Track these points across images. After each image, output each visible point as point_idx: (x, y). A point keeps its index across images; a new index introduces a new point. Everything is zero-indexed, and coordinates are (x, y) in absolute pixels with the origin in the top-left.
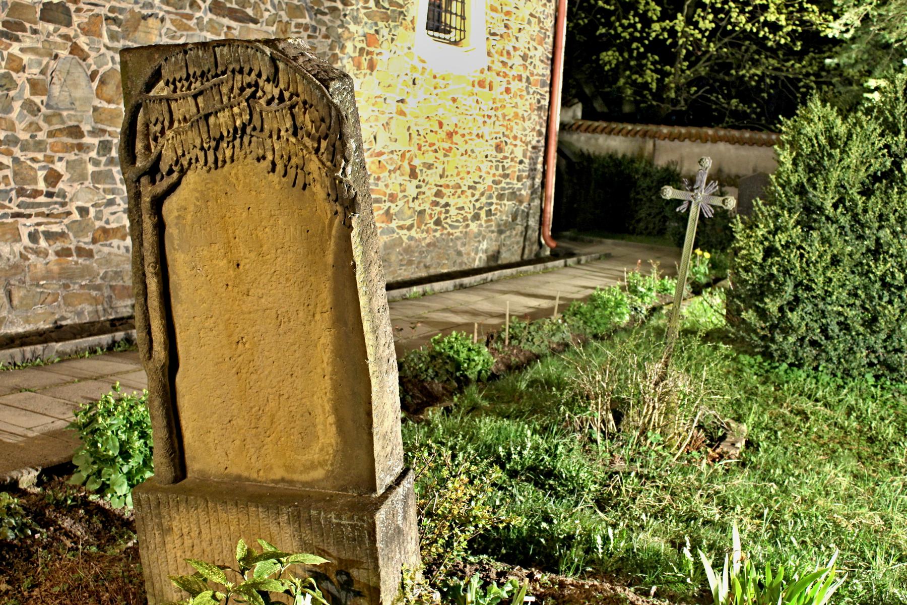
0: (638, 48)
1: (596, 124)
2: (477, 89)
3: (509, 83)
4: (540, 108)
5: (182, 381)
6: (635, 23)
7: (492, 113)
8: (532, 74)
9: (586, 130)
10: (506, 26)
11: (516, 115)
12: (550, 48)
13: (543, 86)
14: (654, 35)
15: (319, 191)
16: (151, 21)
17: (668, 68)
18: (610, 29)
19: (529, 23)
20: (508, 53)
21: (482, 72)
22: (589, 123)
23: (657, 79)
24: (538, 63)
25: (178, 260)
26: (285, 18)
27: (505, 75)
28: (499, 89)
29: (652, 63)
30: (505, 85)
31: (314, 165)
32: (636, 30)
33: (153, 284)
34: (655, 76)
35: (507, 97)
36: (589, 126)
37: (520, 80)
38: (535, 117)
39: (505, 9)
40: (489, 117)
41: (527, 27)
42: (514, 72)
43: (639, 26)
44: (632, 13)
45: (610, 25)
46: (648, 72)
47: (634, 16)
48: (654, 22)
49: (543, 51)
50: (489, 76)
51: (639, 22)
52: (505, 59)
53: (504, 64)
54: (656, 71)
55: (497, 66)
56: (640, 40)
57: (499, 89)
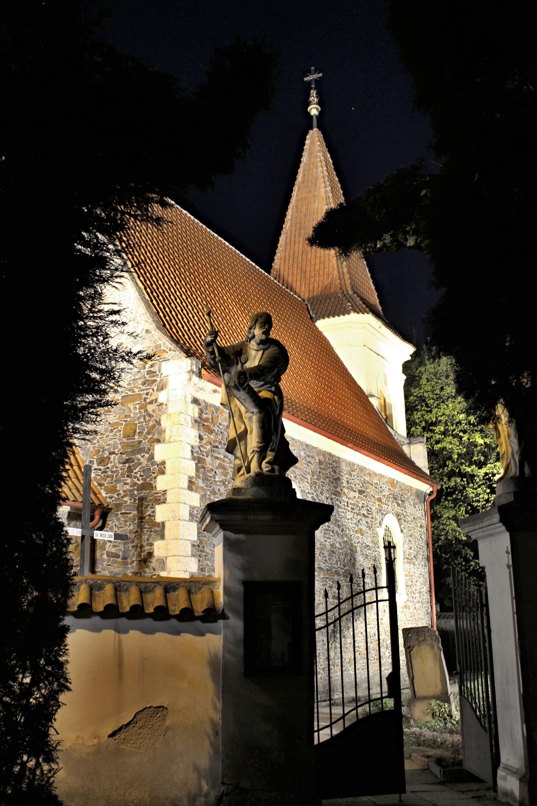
0: (465, 575)
1: (448, 614)
2: (404, 610)
3: (415, 605)
4: (428, 613)
5: (414, 681)
6: (462, 562)
7: (411, 619)
8: (423, 599)
9: (444, 618)
10: (412, 581)
11: (419, 618)
12: (428, 586)
13: (428, 603)
14: (472, 568)
15: (436, 648)
16: (321, 605)
17: (481, 583)
18: (449, 565)
19: (420, 577)
20: (414, 592)
21: (405, 602)
22: (445, 614)
23: (477, 589)
24: (425, 594)
25: (414, 662)
27: (414, 602)
28: (412, 608)
29: (473, 581)
30: (414, 606)
31: (435, 644)
32: (463, 566)
33: (410, 665)
34: (476, 588)
35: (415, 611)
36: (445, 615)
37: (419, 603)
38: (426, 618)
39: (411, 574)
40: (410, 621)
41: (419, 579)
42: (416, 600)
43: (464, 563)
44: (459, 557)
45: (449, 564)
46: (472, 586)
47: (460, 558)
48: (471, 561)
49: (426, 588)
50: (409, 604)
51: (464, 561)
52: (412, 595)
53: (413, 597)
54: (475, 585)
55: (410, 599)
56: (466, 570)
57: (412, 608)
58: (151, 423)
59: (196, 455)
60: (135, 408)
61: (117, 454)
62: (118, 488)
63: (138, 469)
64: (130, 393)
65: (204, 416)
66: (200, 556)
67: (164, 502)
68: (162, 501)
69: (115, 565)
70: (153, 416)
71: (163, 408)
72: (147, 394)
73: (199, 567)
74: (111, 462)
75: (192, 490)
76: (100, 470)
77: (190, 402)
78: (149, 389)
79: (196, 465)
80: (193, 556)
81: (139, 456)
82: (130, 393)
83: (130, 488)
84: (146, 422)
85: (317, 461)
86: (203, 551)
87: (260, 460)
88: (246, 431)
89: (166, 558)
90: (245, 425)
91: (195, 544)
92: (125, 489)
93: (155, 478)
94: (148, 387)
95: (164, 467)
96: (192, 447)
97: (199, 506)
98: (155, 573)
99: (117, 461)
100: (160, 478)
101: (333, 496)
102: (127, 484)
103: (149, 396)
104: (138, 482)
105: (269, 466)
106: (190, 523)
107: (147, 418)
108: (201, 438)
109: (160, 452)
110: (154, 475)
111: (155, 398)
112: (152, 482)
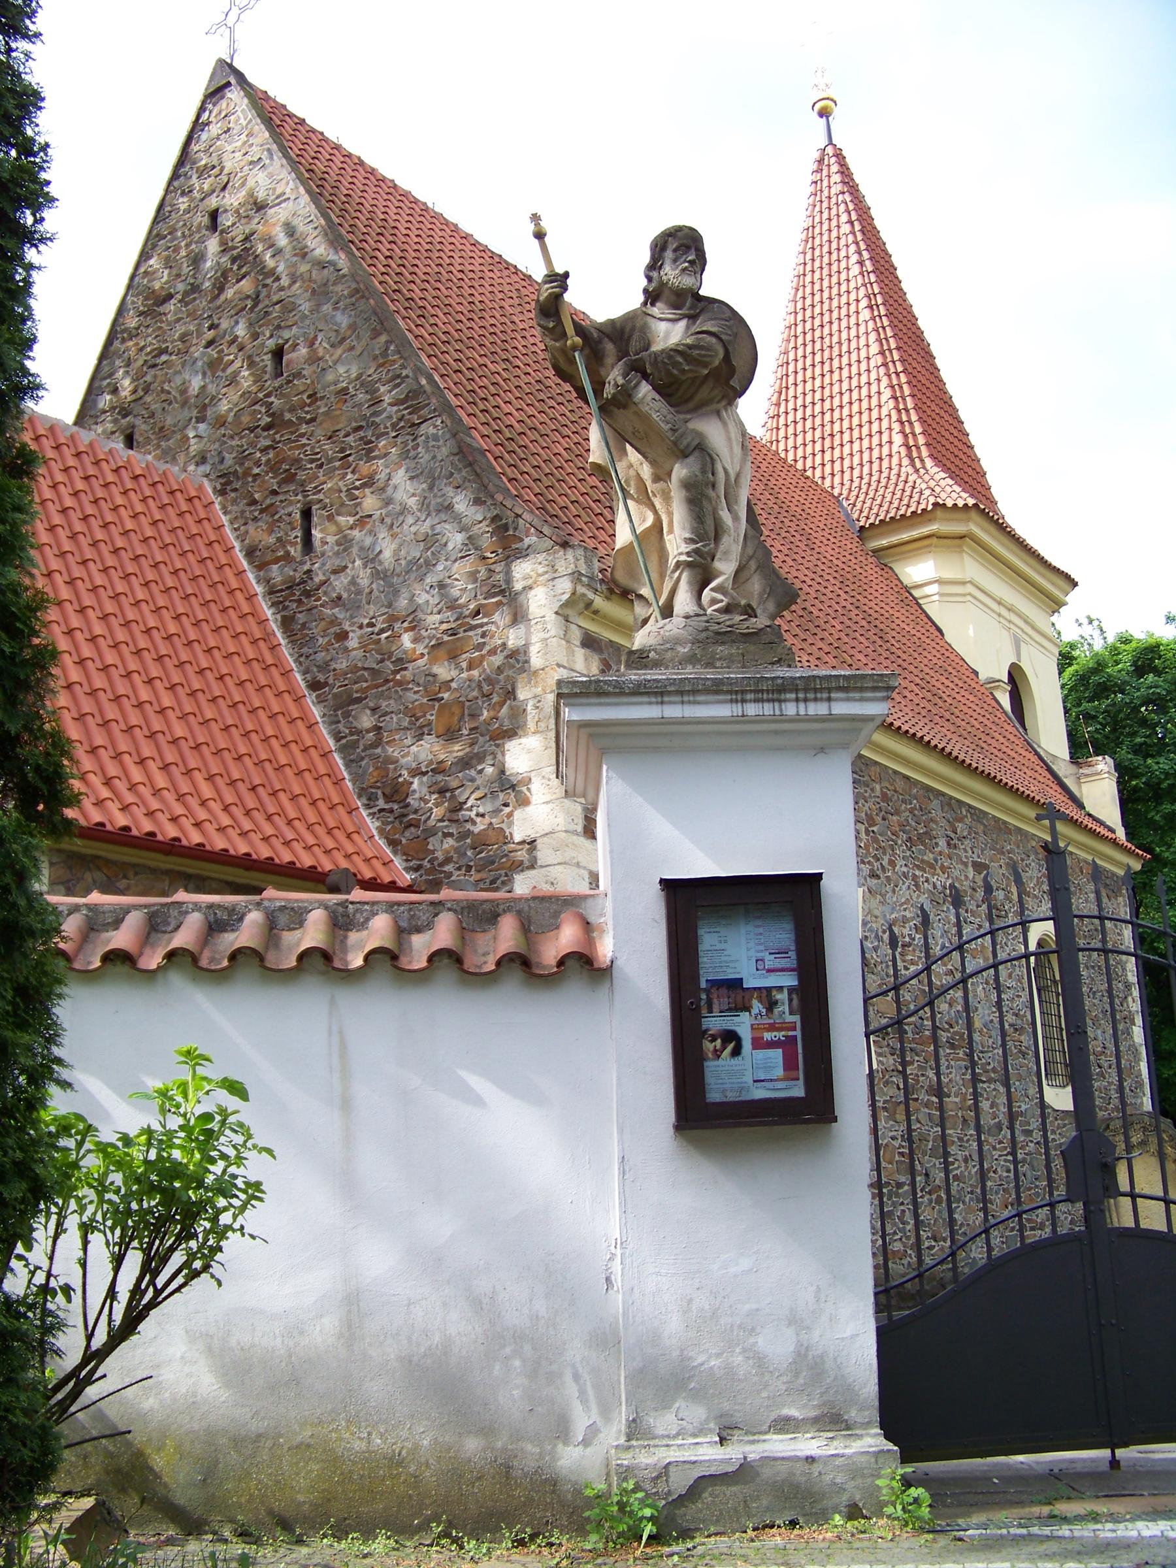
26: (964, 1091)
61: (424, 774)
62: (430, 847)
64: (446, 638)
67: (532, 867)
68: (527, 864)
70: (498, 682)
71: (518, 661)
72: (483, 635)
74: (414, 791)
76: (391, 811)
77: (578, 643)
78: (487, 624)
82: (446, 638)
83: (456, 845)
84: (484, 696)
85: (878, 793)
87: (697, 588)
88: (658, 527)
90: (656, 512)
92: (446, 846)
93: (510, 815)
94: (485, 620)
95: (529, 789)
101: (917, 873)
102: (451, 835)
103: (487, 639)
104: (472, 828)
105: (719, 596)
107: (486, 688)
110: (507, 810)
111: (500, 642)
112: (503, 826)
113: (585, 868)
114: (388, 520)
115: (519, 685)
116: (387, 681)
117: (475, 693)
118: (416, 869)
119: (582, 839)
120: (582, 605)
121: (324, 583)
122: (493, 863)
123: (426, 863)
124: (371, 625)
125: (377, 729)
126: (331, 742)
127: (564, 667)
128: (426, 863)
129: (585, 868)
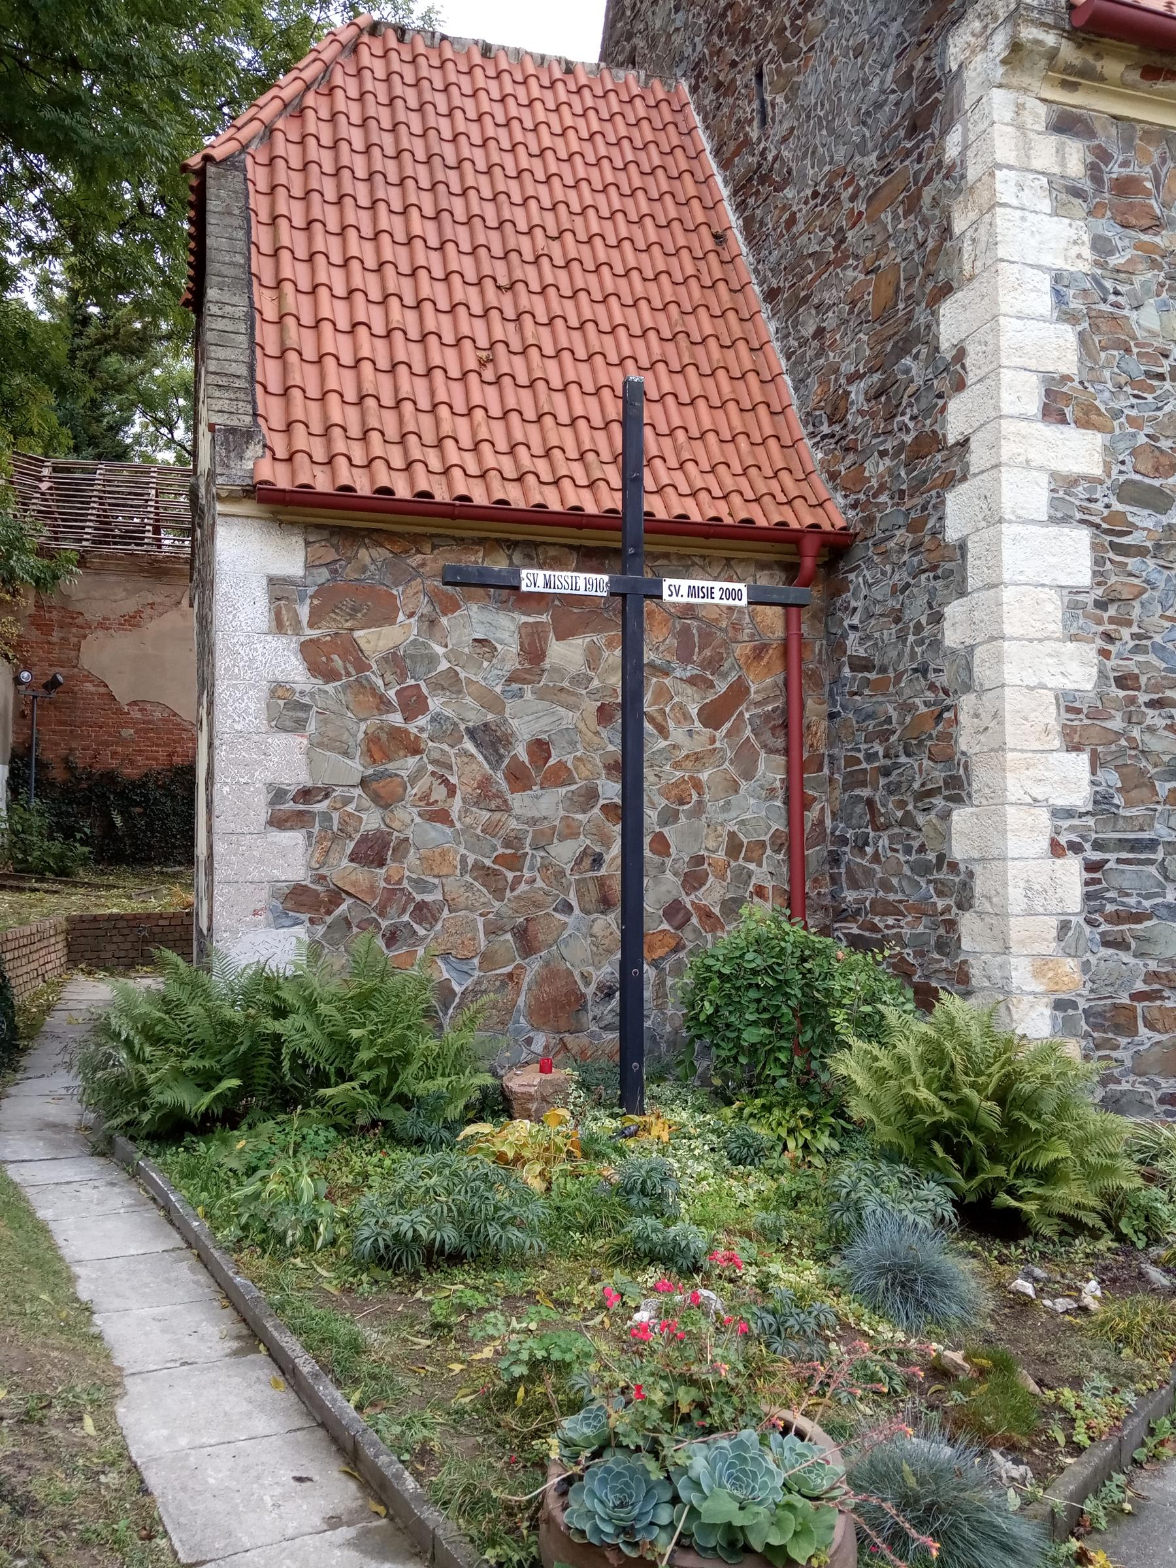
58: (931, 244)
59: (1076, 304)
60: (896, 218)
63: (905, 401)
64: (883, 180)
65: (1115, 170)
66: (1109, 637)
67: (964, 478)
69: (866, 692)
73: (1102, 674)
75: (1063, 421)
77: (1041, 127)
79: (1082, 338)
80: (1074, 638)
81: (907, 361)
86: (1129, 623)
89: (971, 649)
91: (1080, 598)
95: (963, 367)
96: (1057, 278)
97: (1097, 471)
98: (948, 702)
99: (861, 398)
100: (953, 405)
106: (1054, 530)
108: (1101, 246)
109: (952, 322)
110: (941, 402)
112: (936, 427)
113: (1041, 468)
114: (828, 44)
115: (956, 215)
116: (829, 264)
117: (911, 247)
118: (854, 506)
119: (1040, 426)
120: (1043, 63)
121: (775, 159)
122: (925, 481)
123: (862, 496)
124: (815, 194)
125: (820, 332)
126: (783, 362)
127: (1010, 168)
128: (862, 496)
129: (1041, 468)
